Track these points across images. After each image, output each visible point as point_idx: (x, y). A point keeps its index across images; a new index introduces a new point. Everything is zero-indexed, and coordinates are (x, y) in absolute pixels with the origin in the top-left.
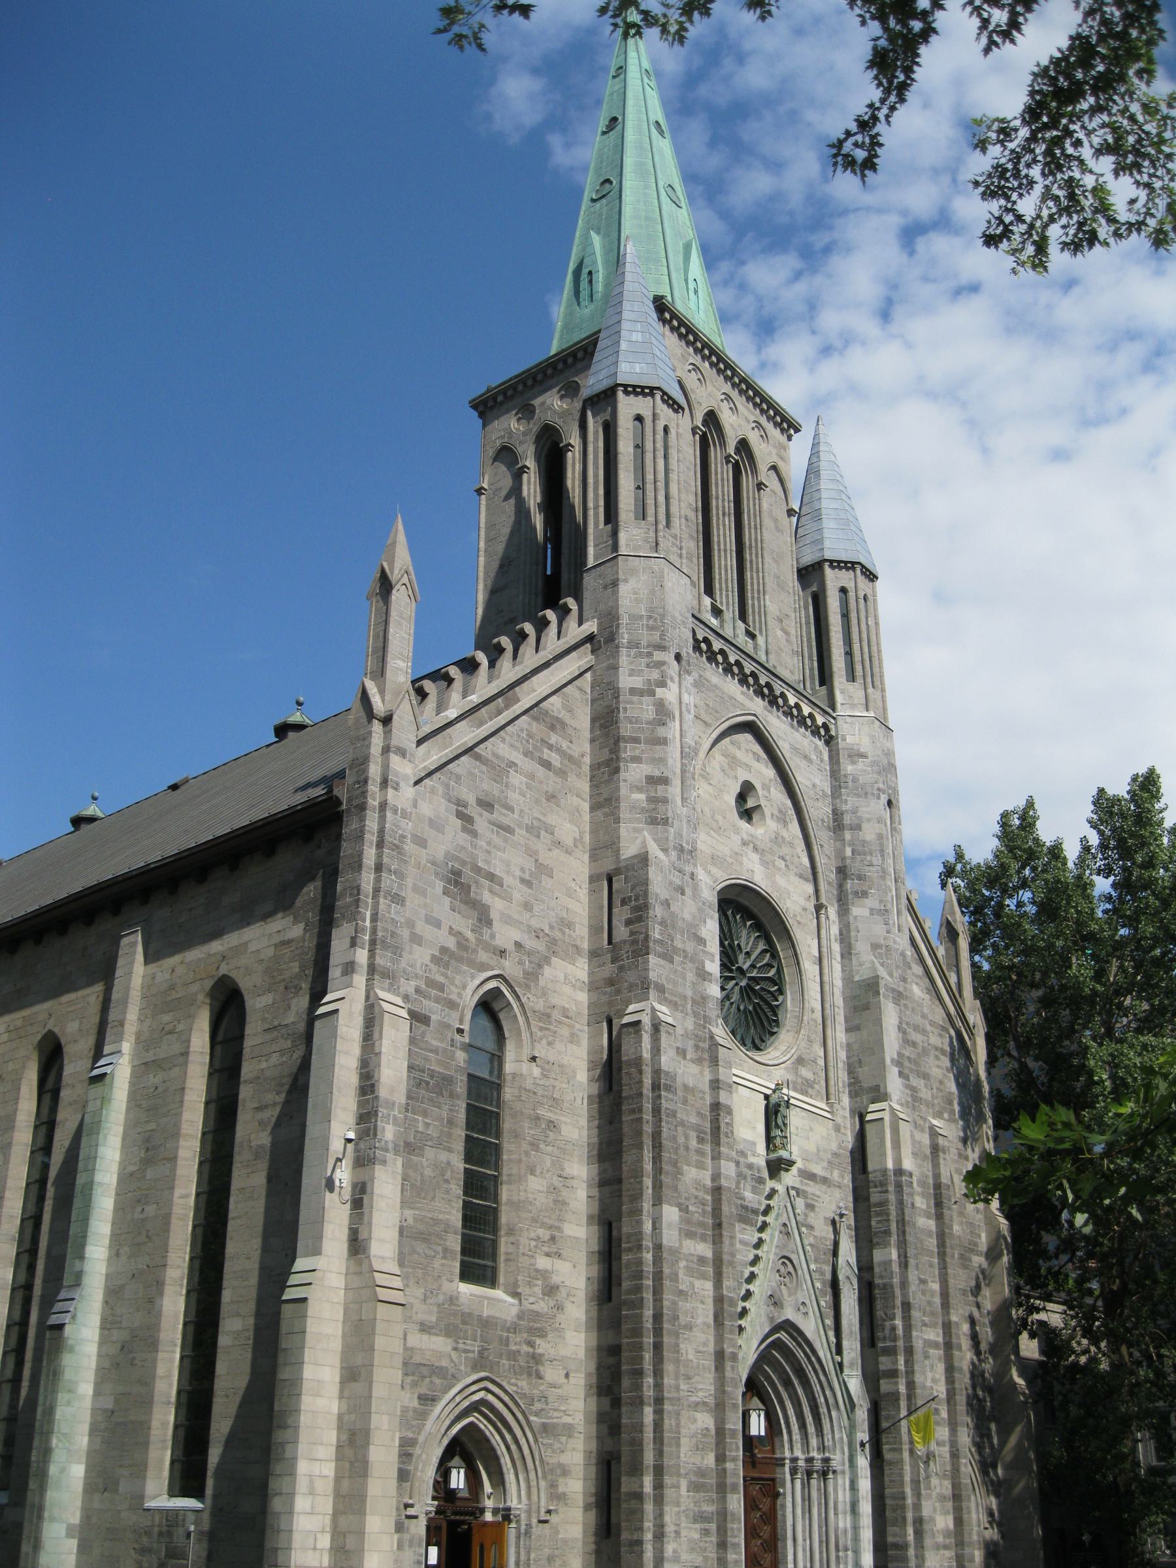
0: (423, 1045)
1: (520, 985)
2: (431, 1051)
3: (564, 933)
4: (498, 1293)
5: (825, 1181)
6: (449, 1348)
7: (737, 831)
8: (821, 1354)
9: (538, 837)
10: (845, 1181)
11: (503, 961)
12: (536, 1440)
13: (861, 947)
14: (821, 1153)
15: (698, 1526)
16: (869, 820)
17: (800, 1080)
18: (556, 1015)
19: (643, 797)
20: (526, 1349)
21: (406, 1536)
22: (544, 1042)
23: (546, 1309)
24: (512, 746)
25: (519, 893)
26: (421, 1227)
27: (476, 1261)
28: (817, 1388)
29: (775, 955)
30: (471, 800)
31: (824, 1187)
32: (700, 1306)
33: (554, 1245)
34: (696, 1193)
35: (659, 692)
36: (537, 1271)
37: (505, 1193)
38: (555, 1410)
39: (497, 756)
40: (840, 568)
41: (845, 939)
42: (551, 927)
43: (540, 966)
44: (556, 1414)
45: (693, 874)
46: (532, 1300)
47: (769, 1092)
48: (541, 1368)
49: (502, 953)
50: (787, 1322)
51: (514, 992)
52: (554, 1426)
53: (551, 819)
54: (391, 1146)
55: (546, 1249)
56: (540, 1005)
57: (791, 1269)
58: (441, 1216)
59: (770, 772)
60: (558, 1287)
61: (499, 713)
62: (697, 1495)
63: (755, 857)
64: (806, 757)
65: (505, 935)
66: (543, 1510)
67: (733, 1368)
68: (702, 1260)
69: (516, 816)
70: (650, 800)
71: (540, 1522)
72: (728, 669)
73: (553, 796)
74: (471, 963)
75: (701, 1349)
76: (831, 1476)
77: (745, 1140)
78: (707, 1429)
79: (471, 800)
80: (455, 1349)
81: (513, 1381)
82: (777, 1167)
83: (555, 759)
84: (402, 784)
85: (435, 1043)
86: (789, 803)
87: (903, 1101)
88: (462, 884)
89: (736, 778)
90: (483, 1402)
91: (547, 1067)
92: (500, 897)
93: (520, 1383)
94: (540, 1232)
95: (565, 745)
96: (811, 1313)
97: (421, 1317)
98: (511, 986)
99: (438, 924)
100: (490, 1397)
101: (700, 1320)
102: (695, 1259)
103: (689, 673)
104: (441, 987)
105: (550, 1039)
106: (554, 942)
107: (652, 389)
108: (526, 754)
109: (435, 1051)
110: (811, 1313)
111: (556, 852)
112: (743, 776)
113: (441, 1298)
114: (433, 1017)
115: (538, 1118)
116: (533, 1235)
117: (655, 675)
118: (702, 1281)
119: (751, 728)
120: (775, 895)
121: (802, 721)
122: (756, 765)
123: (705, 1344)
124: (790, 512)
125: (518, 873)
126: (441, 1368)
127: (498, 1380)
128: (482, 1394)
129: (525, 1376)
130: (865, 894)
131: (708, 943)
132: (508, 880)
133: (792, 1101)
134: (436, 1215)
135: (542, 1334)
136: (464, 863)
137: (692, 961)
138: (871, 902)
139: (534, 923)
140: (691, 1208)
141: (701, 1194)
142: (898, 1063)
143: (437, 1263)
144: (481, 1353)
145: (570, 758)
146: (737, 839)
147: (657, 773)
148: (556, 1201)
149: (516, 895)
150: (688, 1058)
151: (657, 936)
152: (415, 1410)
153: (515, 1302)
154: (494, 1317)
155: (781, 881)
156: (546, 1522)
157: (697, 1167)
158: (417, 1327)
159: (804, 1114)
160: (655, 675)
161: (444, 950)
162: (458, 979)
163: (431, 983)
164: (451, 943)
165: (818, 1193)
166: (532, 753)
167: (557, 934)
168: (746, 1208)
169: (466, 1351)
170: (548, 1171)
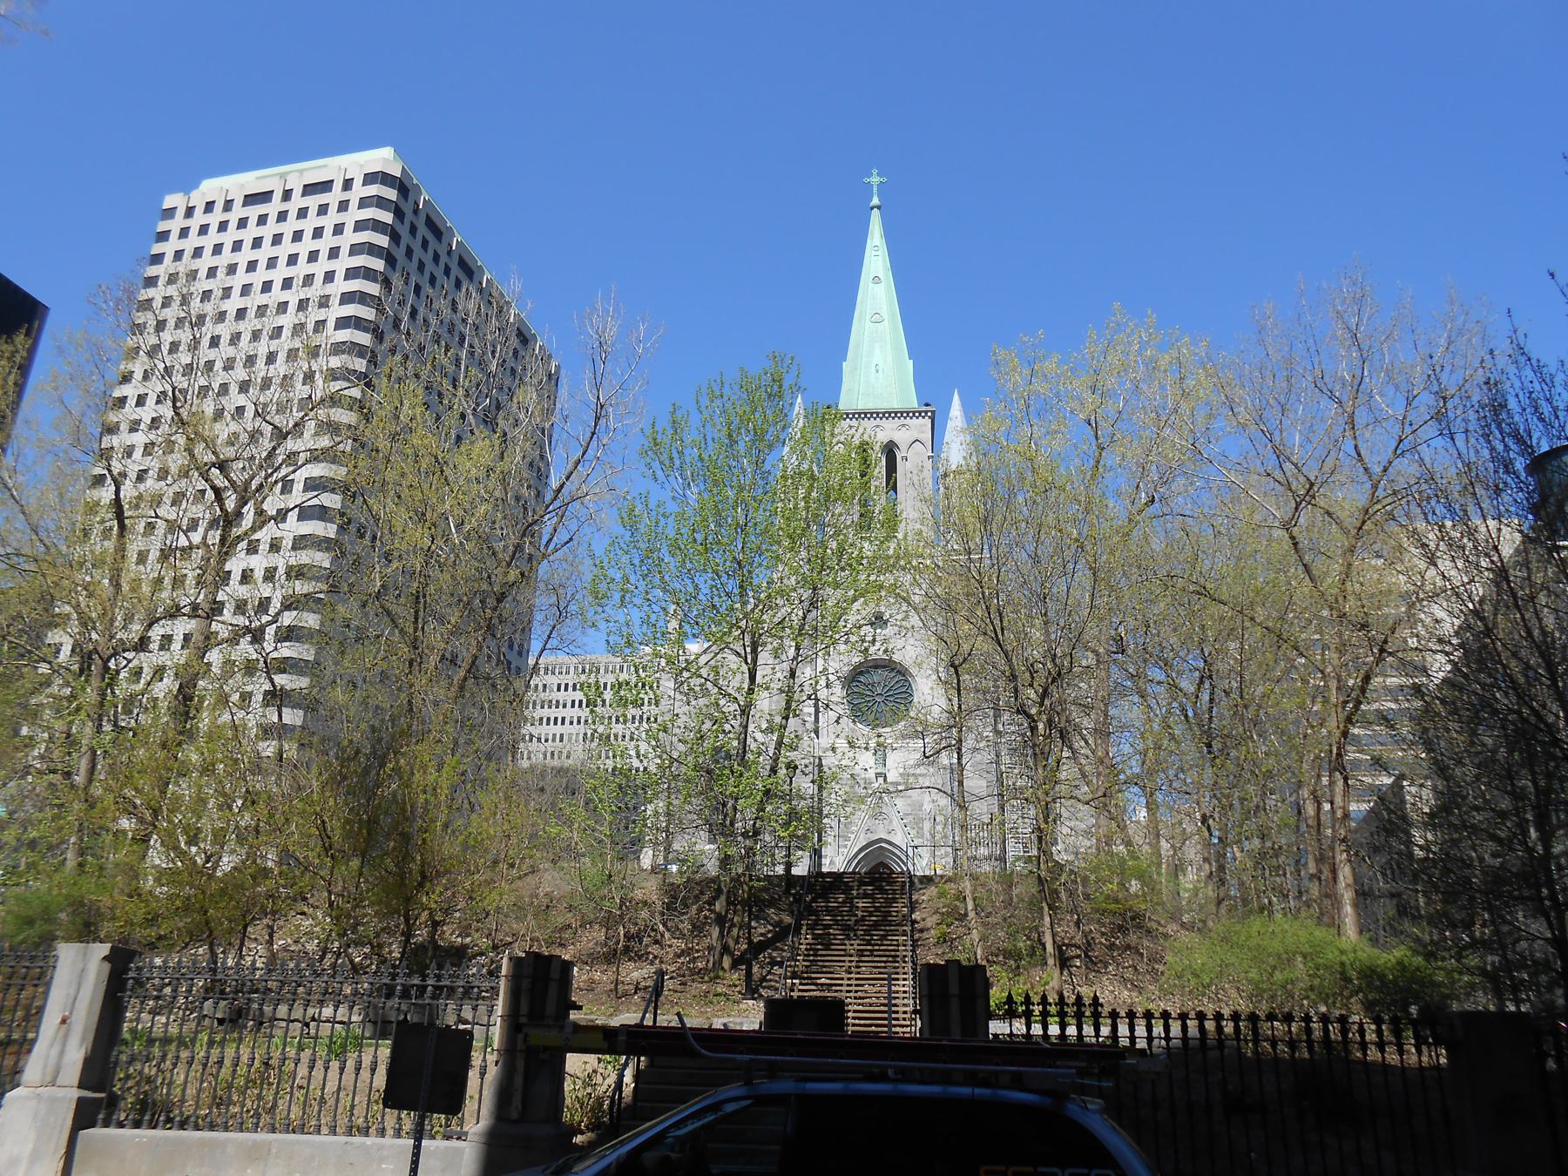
29: (907, 681)
82: (878, 775)
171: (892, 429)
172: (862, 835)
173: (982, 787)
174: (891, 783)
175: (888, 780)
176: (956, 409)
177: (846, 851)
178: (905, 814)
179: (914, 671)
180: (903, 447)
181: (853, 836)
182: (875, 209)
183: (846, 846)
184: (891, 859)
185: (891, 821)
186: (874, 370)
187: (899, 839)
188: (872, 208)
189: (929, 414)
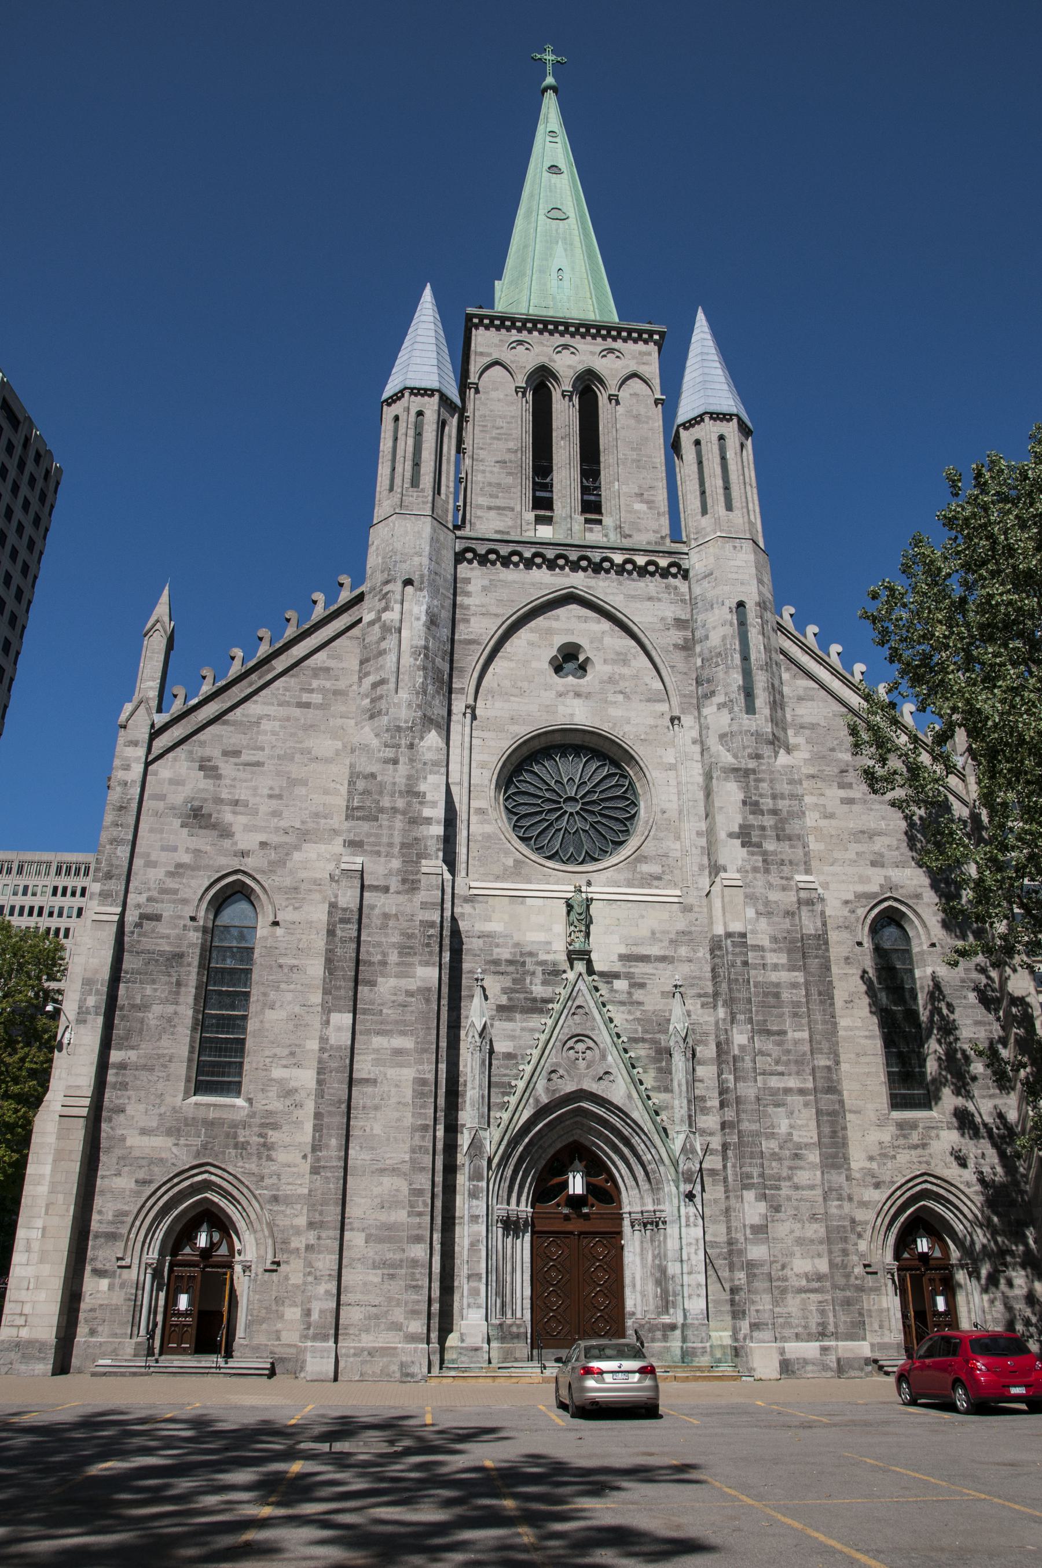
0: (155, 935)
1: (263, 872)
2: (163, 938)
3: (318, 823)
4: (240, 1102)
5: (663, 959)
6: (170, 1145)
7: (547, 687)
8: (635, 1115)
9: (292, 759)
10: (700, 954)
11: (246, 859)
12: (262, 1208)
13: (713, 741)
14: (657, 935)
15: (379, 1272)
16: (714, 628)
17: (639, 876)
18: (303, 886)
19: (368, 700)
20: (255, 1139)
21: (117, 1281)
22: (291, 908)
23: (281, 1107)
24: (265, 704)
25: (266, 807)
26: (142, 1061)
27: (226, 1079)
28: (641, 1148)
30: (216, 753)
31: (661, 965)
32: (393, 1090)
33: (294, 1058)
34: (394, 998)
35: (385, 616)
36: (272, 1080)
37: (252, 1025)
38: (289, 1184)
39: (247, 716)
40: (693, 426)
41: (701, 741)
42: (303, 822)
43: (287, 854)
44: (290, 1187)
45: (411, 746)
46: (264, 1102)
47: (569, 895)
48: (273, 1154)
49: (243, 854)
50: (581, 1090)
51: (254, 879)
52: (286, 1196)
53: (309, 743)
54: (92, 1010)
55: (284, 1062)
56: (288, 882)
57: (591, 1044)
58: (166, 1052)
59: (606, 625)
60: (296, 1090)
61: (251, 685)
62: (380, 1246)
63: (577, 702)
64: (650, 599)
65: (246, 840)
66: (269, 1262)
67: (423, 1137)
68: (398, 1052)
69: (267, 751)
70: (373, 701)
71: (266, 1271)
72: (529, 564)
73: (311, 726)
74: (207, 867)
75: (394, 1124)
76: (661, 1226)
77: (533, 942)
78: (397, 1190)
79: (216, 753)
80: (176, 1145)
81: (240, 1164)
82: (573, 956)
83: (316, 698)
84: (134, 765)
85: (168, 931)
86: (633, 643)
87: (748, 867)
88: (203, 815)
89: (551, 645)
90: (205, 1181)
91: (292, 926)
92: (241, 814)
93: (247, 1166)
94: (278, 1051)
95: (328, 684)
96: (620, 1080)
97: (141, 1124)
98: (250, 876)
99: (175, 849)
100: (213, 1178)
101: (393, 1100)
102: (389, 1052)
103: (421, 590)
104: (176, 892)
105: (297, 905)
106: (306, 832)
107: (402, 391)
108: (279, 705)
109: (168, 937)
110: (620, 1080)
111: (313, 766)
112: (559, 640)
113: (163, 1110)
114: (165, 914)
115: (281, 966)
116: (267, 1053)
117: (383, 604)
118: (398, 1069)
119: (570, 598)
120: (605, 727)
121: (643, 572)
122: (584, 626)
123: (398, 1120)
124: (657, 402)
125: (266, 791)
126: (161, 1160)
127: (223, 1166)
128: (205, 1176)
129: (255, 1159)
130: (713, 693)
131: (428, 794)
132: (252, 801)
133: (590, 896)
134: (160, 1052)
135: (275, 1127)
136: (206, 800)
137: (404, 813)
138: (719, 699)
139: (283, 824)
140: (384, 1011)
141: (401, 998)
142: (745, 836)
143: (160, 1086)
144: (205, 1146)
145: (336, 693)
146: (552, 694)
147: (378, 678)
148: (296, 1026)
149: (263, 809)
150: (391, 891)
151: (356, 804)
152: (131, 1191)
153: (245, 1104)
154: (220, 1118)
155: (614, 712)
156: (276, 1271)
157: (396, 977)
158: (137, 1132)
159: (630, 905)
160: (383, 604)
161: (179, 866)
162: (193, 883)
163: (163, 891)
164: (186, 858)
165: (651, 971)
166: (288, 702)
167: (311, 825)
168: (534, 1000)
169: (187, 1145)
170: (290, 1003)
171: (592, 353)
172: (541, 1085)
173: (794, 985)
174: (602, 974)
175: (598, 967)
176: (702, 336)
177: (506, 1116)
178: (630, 1039)
179: (639, 751)
180: (612, 384)
181: (521, 1085)
182: (550, 92)
183: (504, 1106)
184: (600, 1135)
185: (603, 1057)
186: (554, 275)
187: (618, 1092)
188: (545, 90)
189: (656, 337)
